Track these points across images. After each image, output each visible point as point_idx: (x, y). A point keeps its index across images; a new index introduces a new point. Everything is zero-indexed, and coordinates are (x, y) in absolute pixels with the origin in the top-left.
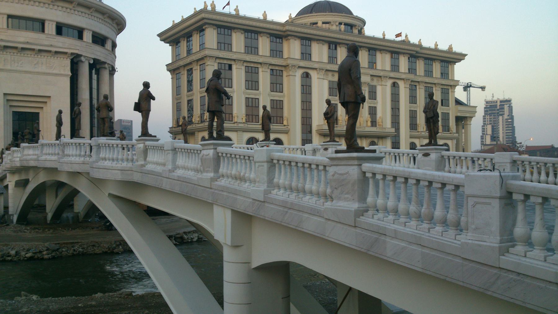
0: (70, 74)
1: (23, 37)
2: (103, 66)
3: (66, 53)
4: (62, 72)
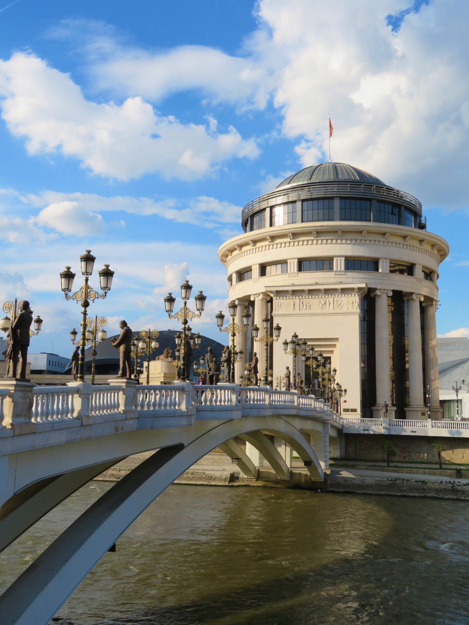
0: (358, 311)
1: (308, 279)
2: (410, 298)
3: (352, 289)
4: (350, 310)
